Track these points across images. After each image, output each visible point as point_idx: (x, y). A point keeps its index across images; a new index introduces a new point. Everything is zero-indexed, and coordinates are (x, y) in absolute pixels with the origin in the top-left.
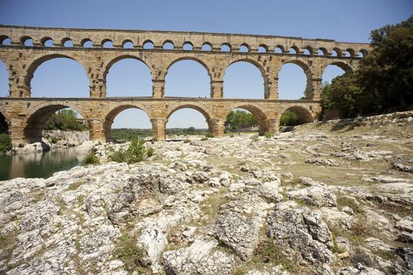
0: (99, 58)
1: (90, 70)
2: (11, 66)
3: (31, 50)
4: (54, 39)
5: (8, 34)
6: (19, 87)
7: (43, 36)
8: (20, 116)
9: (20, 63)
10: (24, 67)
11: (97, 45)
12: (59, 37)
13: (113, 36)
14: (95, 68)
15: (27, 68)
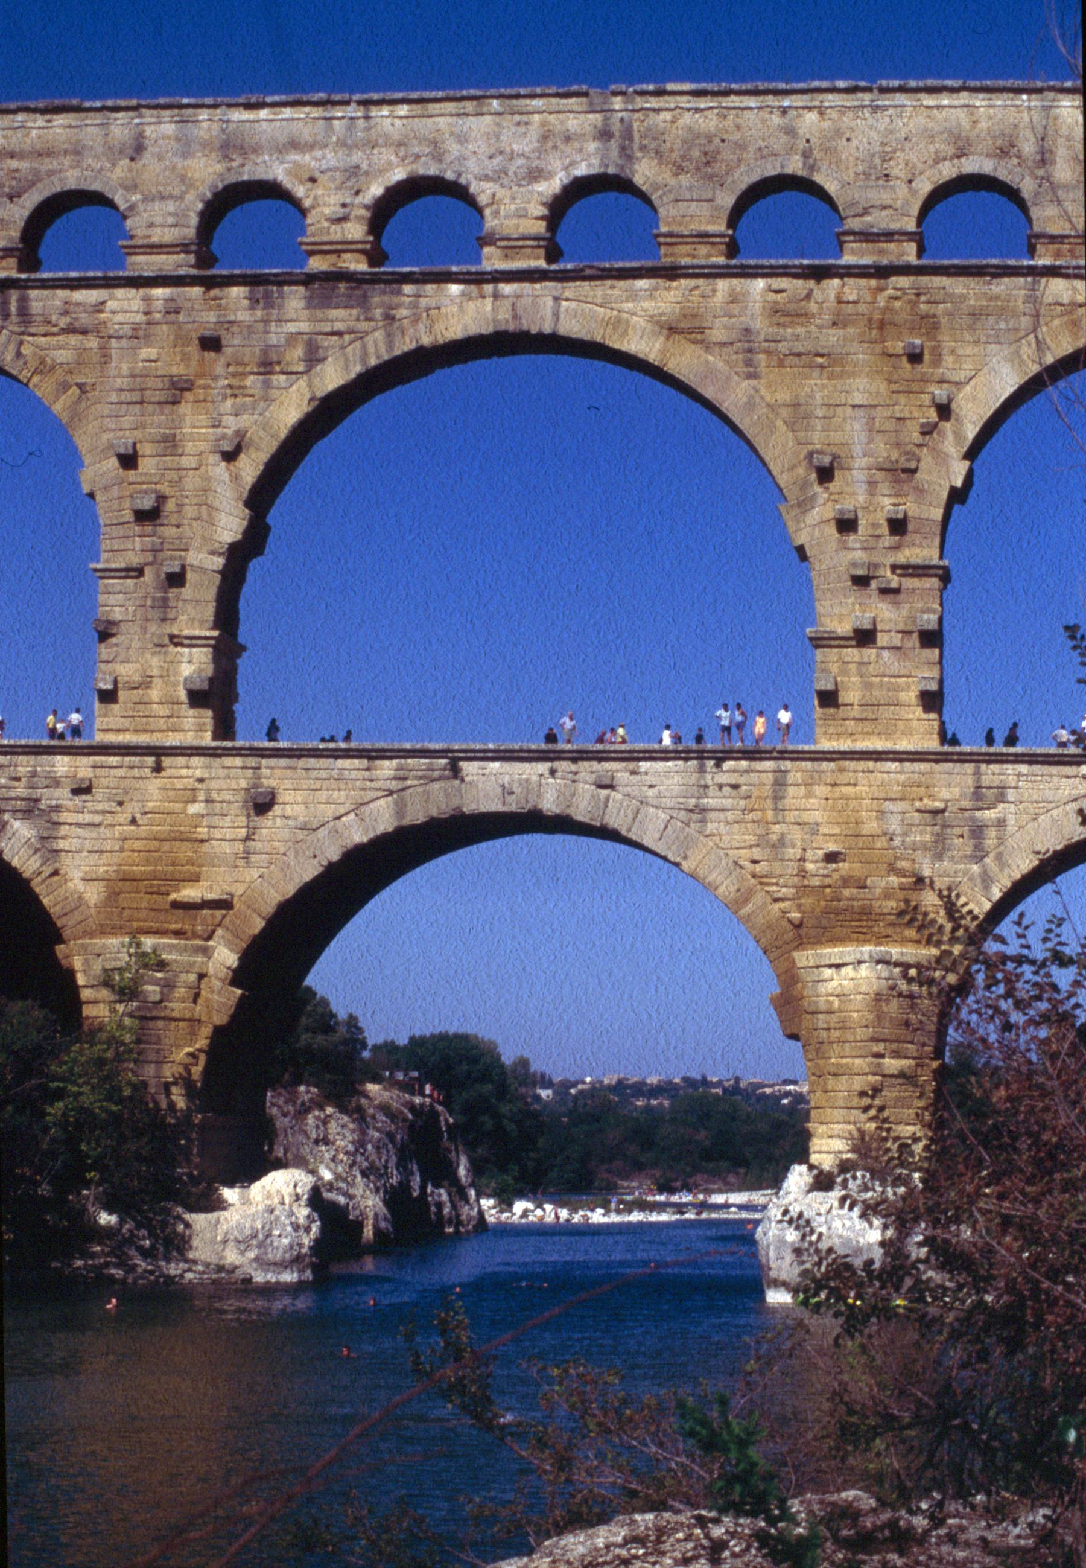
0: (915, 358)
1: (825, 475)
2: (129, 461)
3: (294, 299)
4: (482, 191)
5: (109, 177)
6: (175, 640)
7: (399, 175)
8: (176, 905)
9: (196, 427)
10: (230, 457)
11: (889, 236)
12: (535, 175)
13: (1028, 148)
14: (862, 448)
15: (250, 468)
